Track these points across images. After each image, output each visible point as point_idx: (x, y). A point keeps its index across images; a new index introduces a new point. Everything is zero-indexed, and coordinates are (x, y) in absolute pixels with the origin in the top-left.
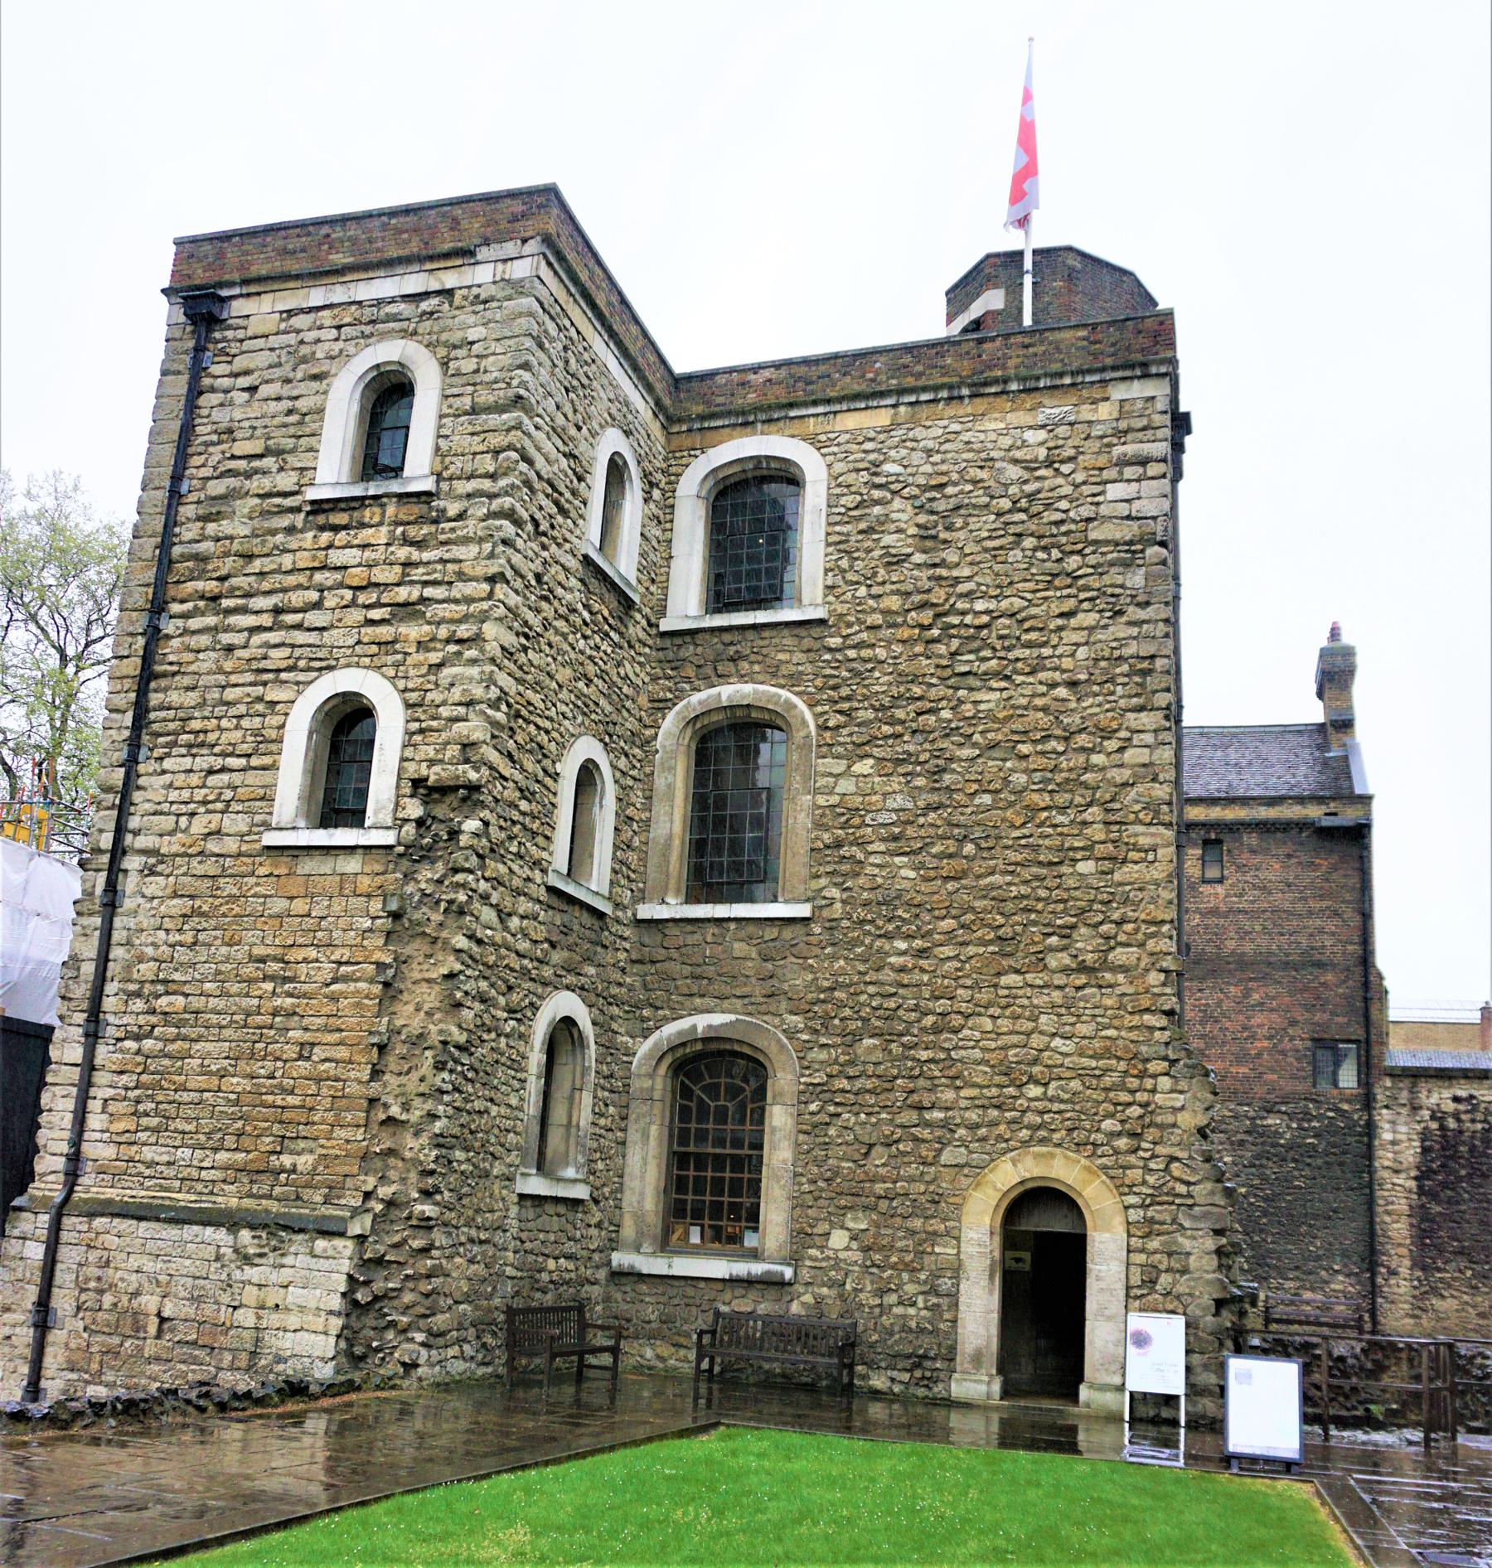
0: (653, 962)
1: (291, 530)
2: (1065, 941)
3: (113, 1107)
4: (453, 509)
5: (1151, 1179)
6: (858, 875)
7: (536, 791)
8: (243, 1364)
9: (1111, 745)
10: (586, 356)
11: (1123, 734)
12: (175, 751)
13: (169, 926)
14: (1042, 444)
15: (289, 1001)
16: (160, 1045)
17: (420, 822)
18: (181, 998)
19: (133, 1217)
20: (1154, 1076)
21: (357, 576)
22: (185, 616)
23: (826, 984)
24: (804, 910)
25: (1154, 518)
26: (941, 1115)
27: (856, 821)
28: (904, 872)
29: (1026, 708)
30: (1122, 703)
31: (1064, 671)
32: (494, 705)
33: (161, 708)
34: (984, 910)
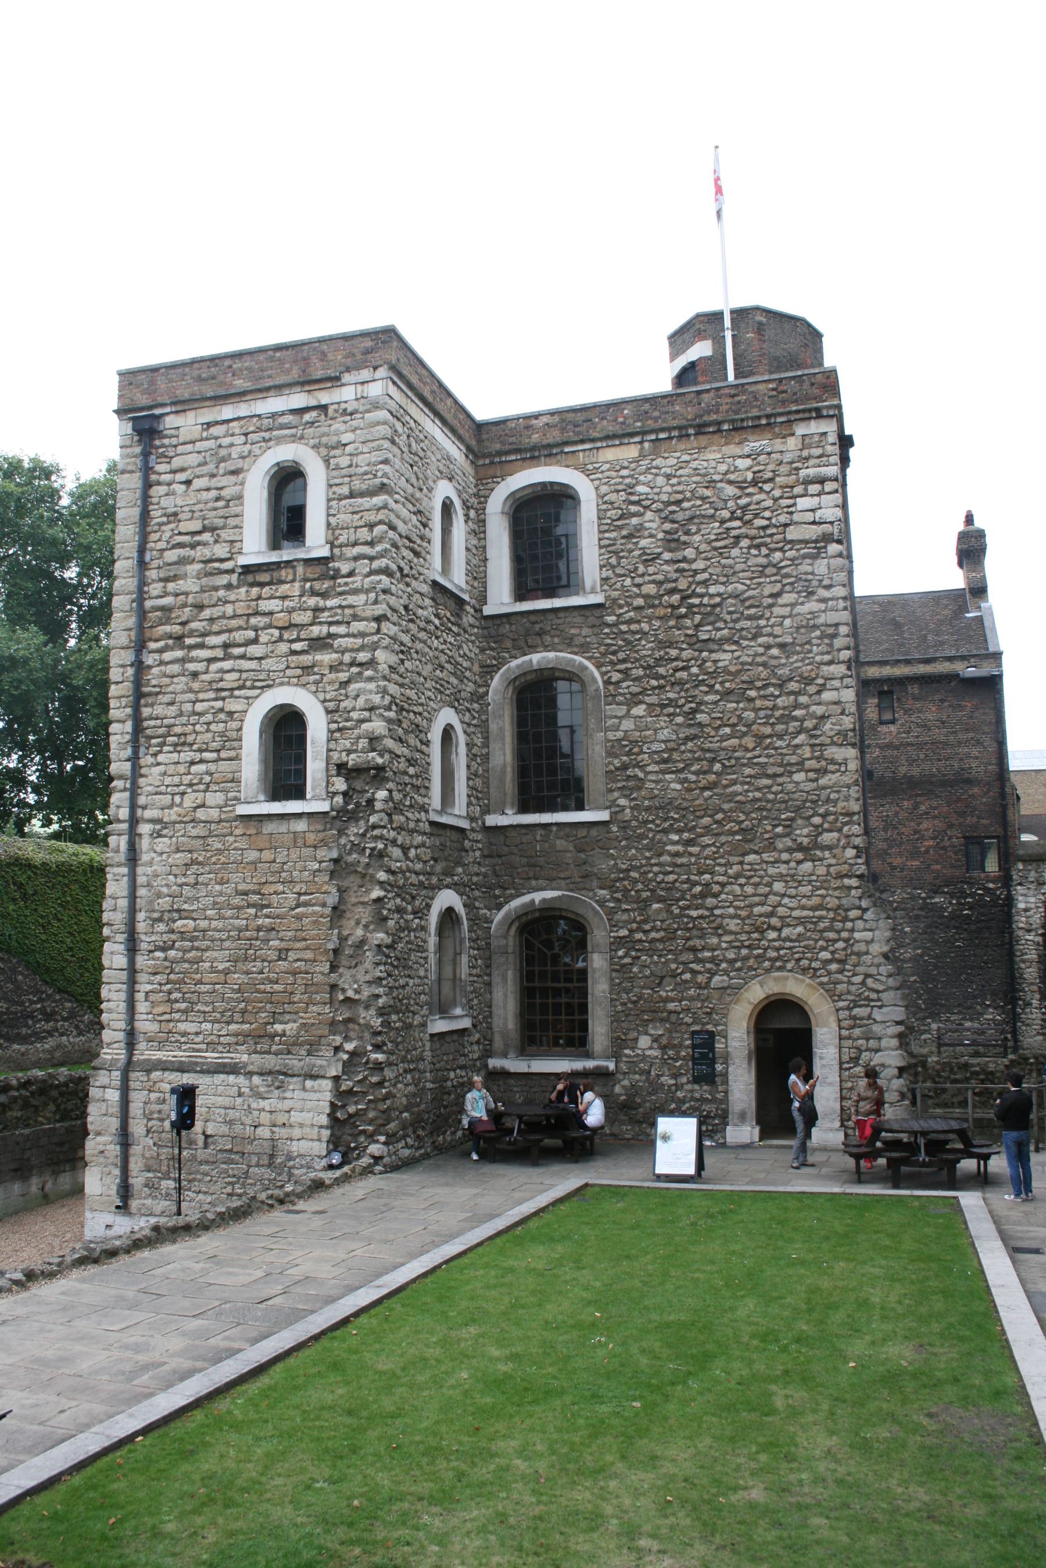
0: (499, 856)
1: (229, 587)
2: (788, 830)
3: (153, 997)
4: (345, 568)
5: (853, 988)
6: (639, 788)
7: (418, 761)
8: (266, 1162)
9: (812, 689)
10: (422, 437)
11: (820, 681)
12: (166, 749)
13: (178, 872)
14: (748, 469)
15: (267, 920)
16: (180, 954)
17: (345, 794)
18: (191, 922)
19: (177, 1070)
20: (852, 920)
21: (281, 619)
22: (161, 651)
23: (624, 867)
24: (603, 816)
25: (831, 523)
26: (708, 954)
27: (636, 750)
28: (673, 786)
29: (750, 664)
30: (818, 658)
31: (776, 636)
32: (389, 709)
33: (151, 718)
34: (731, 810)
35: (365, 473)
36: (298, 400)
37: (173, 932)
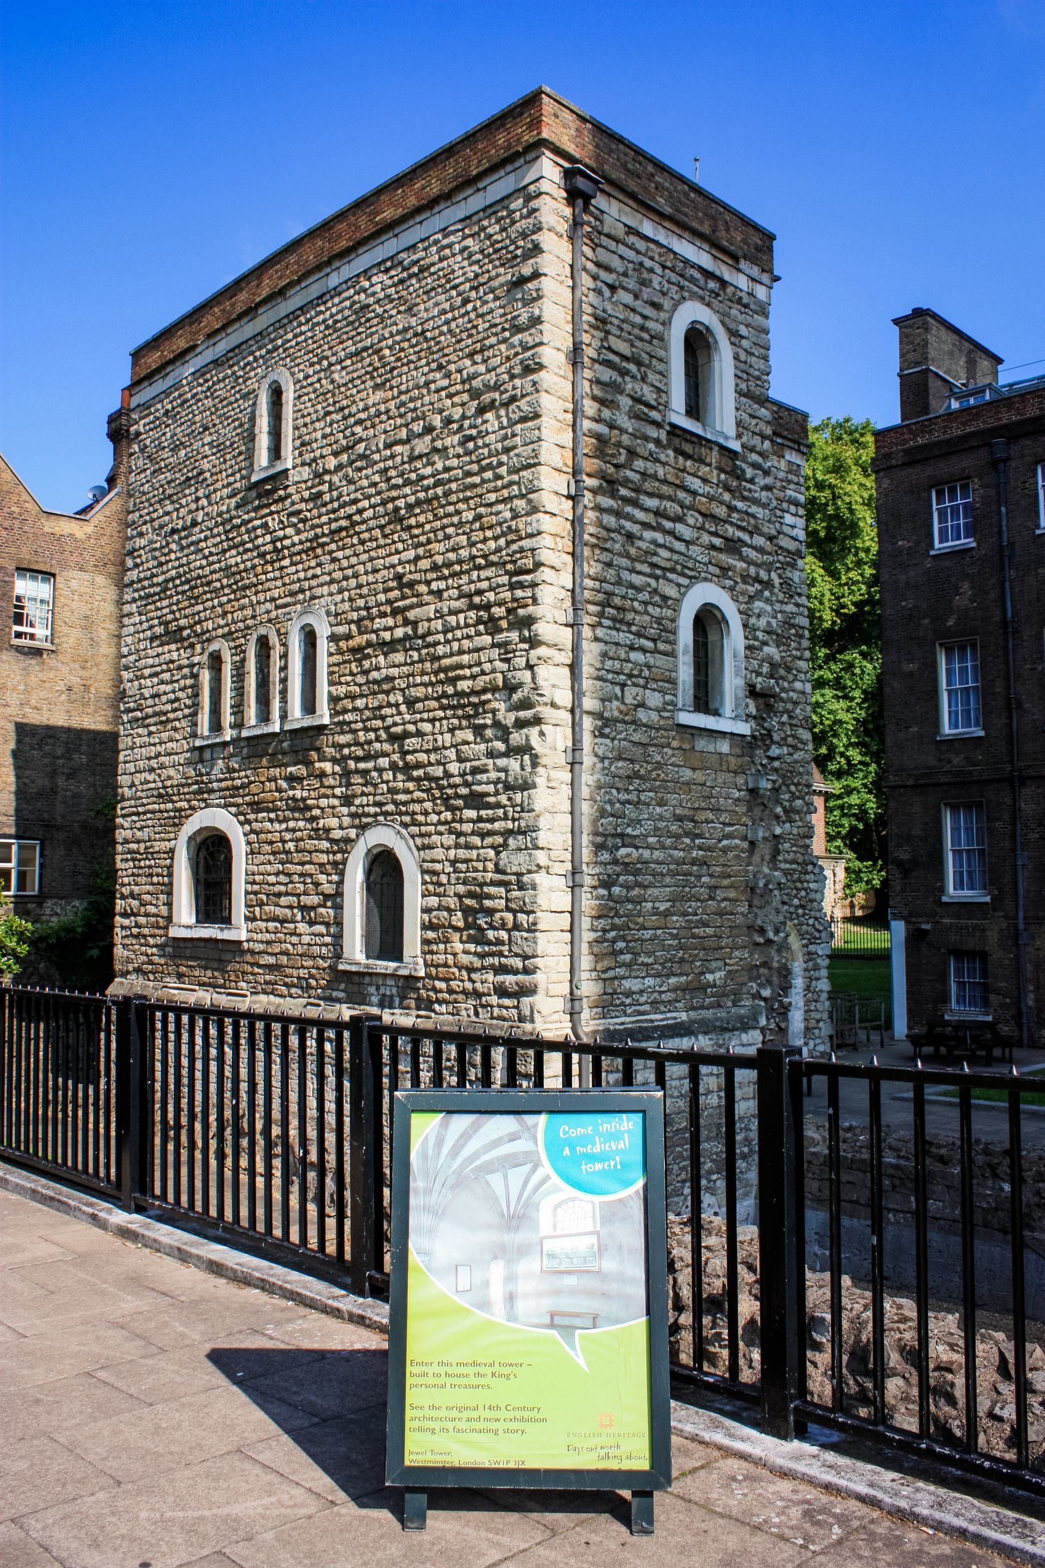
1: (657, 442)
4: (749, 472)
9: (791, 678)
13: (620, 785)
15: (701, 853)
35: (758, 378)
36: (703, 258)
37: (615, 862)
